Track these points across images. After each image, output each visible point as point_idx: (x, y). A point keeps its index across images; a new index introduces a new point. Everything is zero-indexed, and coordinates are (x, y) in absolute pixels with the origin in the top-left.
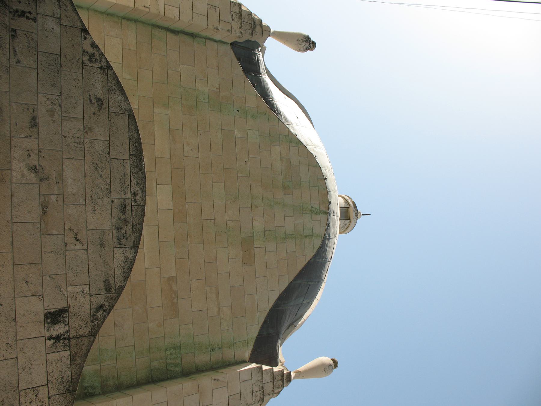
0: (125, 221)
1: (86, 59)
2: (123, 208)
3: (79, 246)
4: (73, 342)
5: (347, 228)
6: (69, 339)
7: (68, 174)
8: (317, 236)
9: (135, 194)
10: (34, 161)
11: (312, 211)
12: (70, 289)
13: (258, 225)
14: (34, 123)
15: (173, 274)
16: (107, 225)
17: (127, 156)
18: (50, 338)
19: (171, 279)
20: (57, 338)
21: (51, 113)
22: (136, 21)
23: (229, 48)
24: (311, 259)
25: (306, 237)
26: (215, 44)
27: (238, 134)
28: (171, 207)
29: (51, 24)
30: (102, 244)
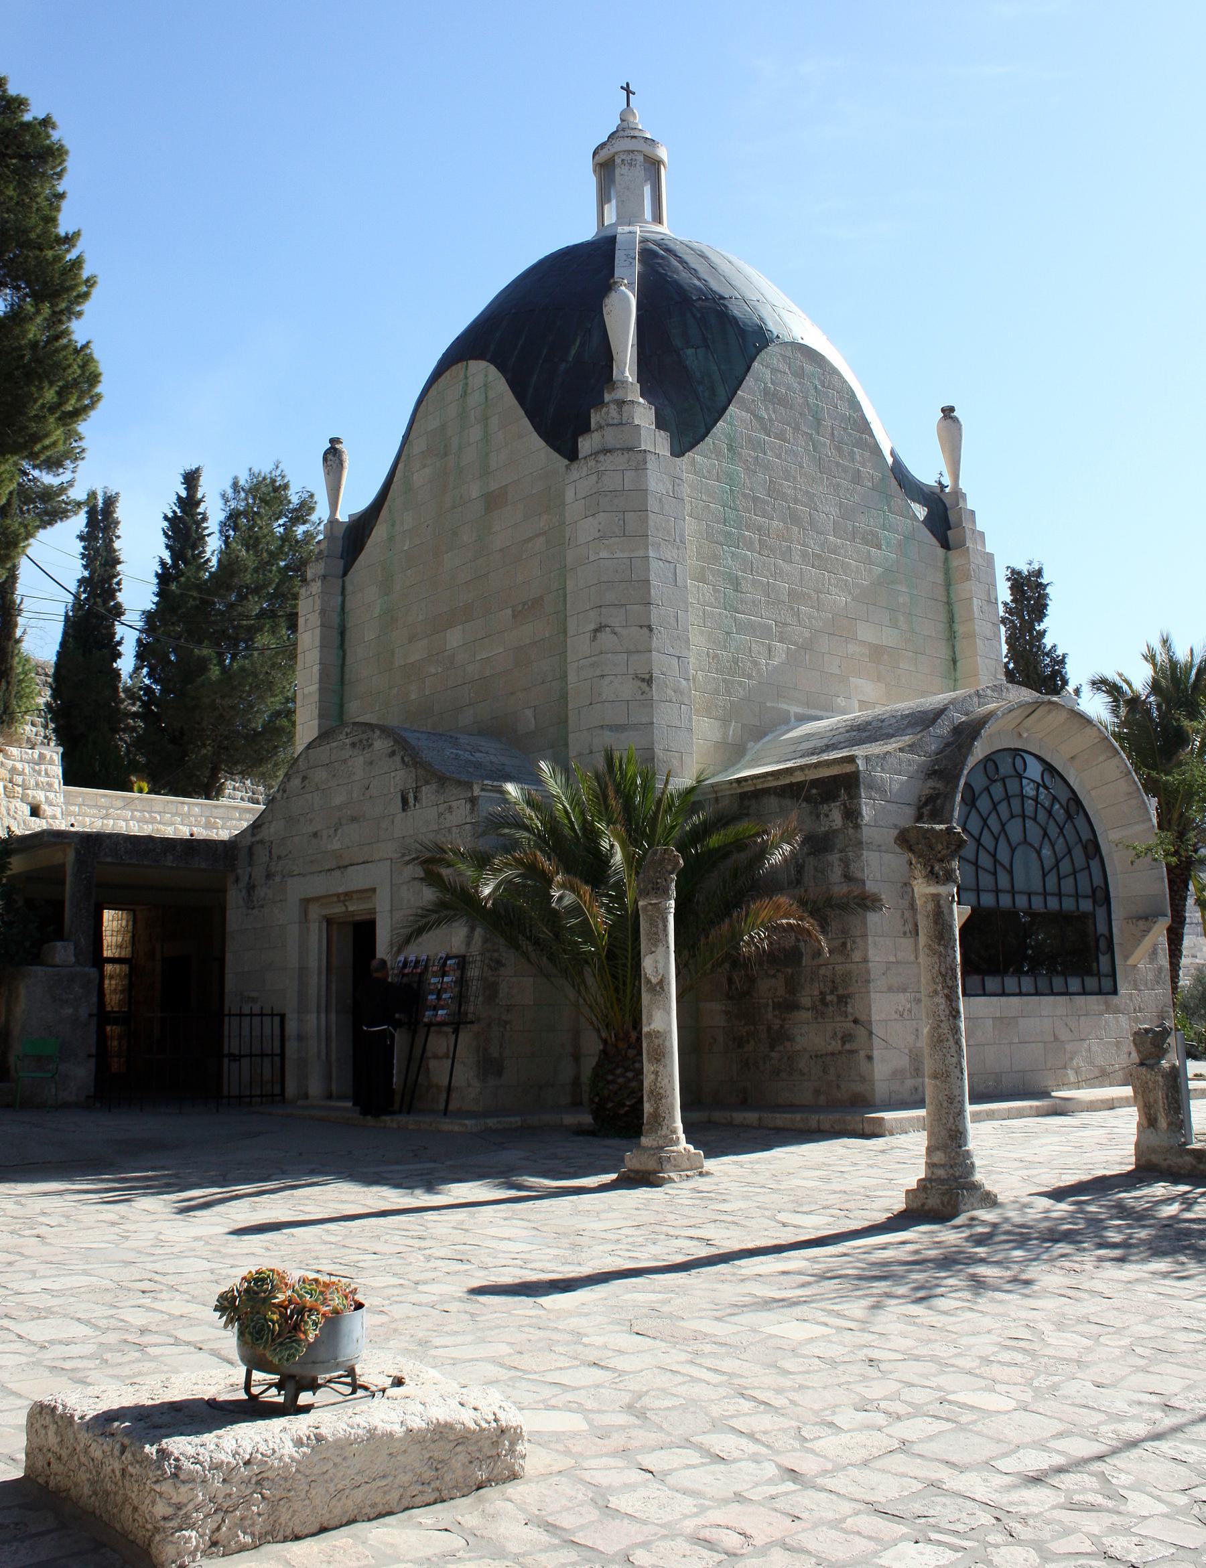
0: (361, 741)
1: (285, 796)
2: (353, 745)
3: (371, 786)
4: (419, 784)
5: (633, 151)
6: (417, 788)
7: (338, 800)
8: (486, 376)
9: (347, 734)
10: (332, 831)
11: (465, 394)
12: (392, 791)
13: (475, 491)
14: (315, 835)
15: (509, 611)
16: (361, 760)
17: (328, 747)
18: (415, 806)
19: (514, 616)
20: (416, 798)
21: (311, 820)
22: (342, 706)
23: (347, 579)
24: (507, 380)
25: (486, 397)
26: (347, 598)
27: (406, 548)
28: (460, 627)
29: (272, 830)
30: (371, 763)
